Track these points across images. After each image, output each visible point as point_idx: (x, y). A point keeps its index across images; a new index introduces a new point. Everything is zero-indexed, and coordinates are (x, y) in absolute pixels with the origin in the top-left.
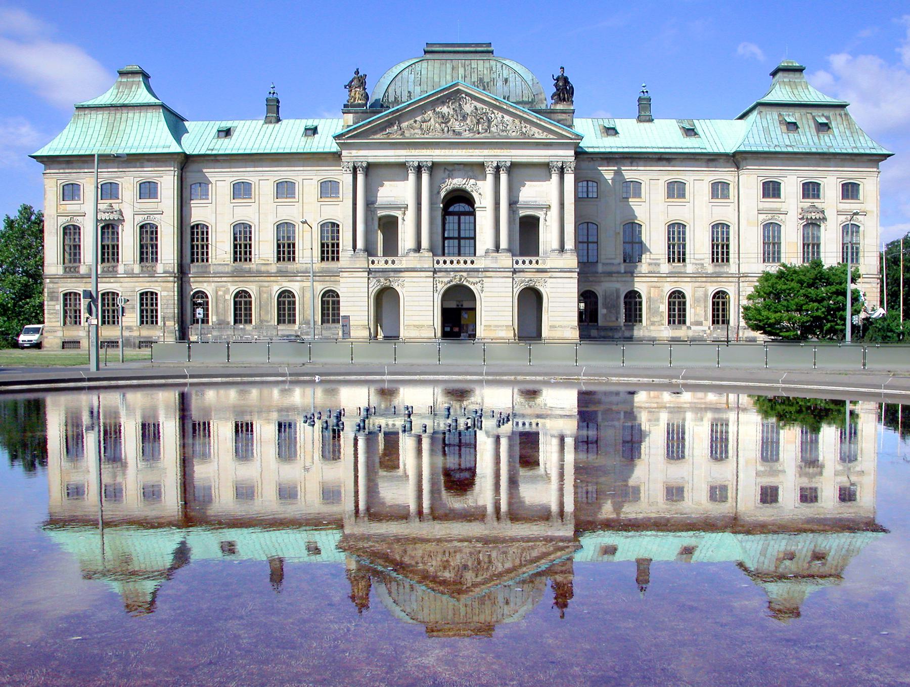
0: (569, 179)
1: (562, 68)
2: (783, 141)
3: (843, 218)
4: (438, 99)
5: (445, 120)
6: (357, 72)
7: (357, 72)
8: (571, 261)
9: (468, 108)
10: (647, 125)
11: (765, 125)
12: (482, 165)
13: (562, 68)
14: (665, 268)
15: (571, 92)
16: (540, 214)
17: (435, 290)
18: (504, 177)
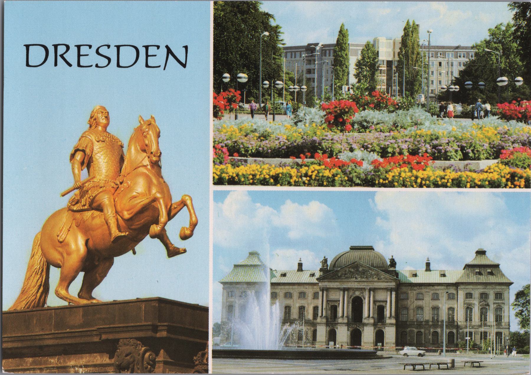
0: (394, 294)
1: (392, 256)
2: (473, 279)
3: (495, 306)
4: (350, 267)
5: (353, 273)
6: (325, 257)
7: (325, 257)
8: (393, 321)
9: (360, 269)
10: (428, 272)
11: (468, 273)
12: (364, 289)
13: (392, 256)
14: (431, 323)
15: (395, 263)
16: (384, 304)
17: (348, 330)
18: (372, 292)
